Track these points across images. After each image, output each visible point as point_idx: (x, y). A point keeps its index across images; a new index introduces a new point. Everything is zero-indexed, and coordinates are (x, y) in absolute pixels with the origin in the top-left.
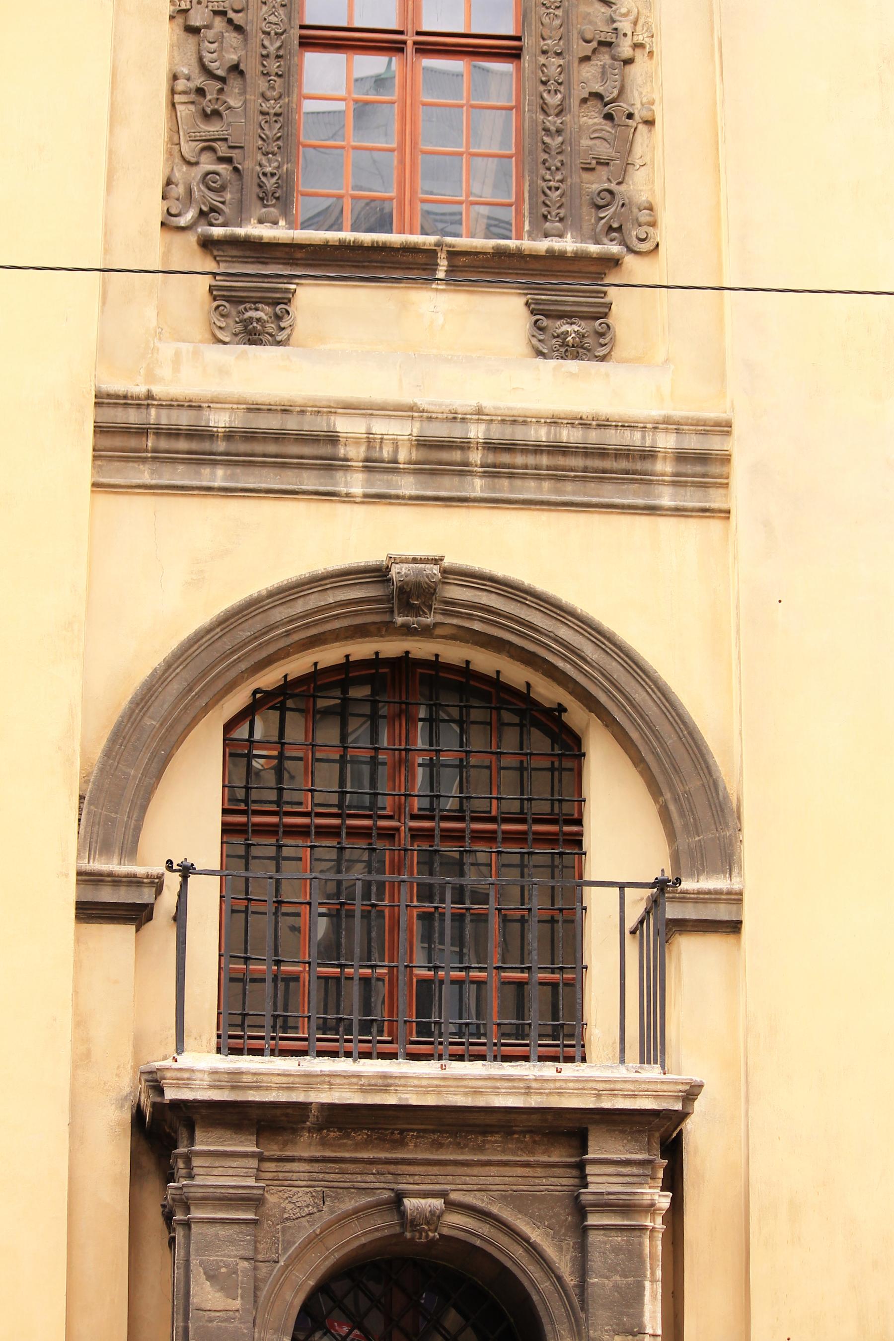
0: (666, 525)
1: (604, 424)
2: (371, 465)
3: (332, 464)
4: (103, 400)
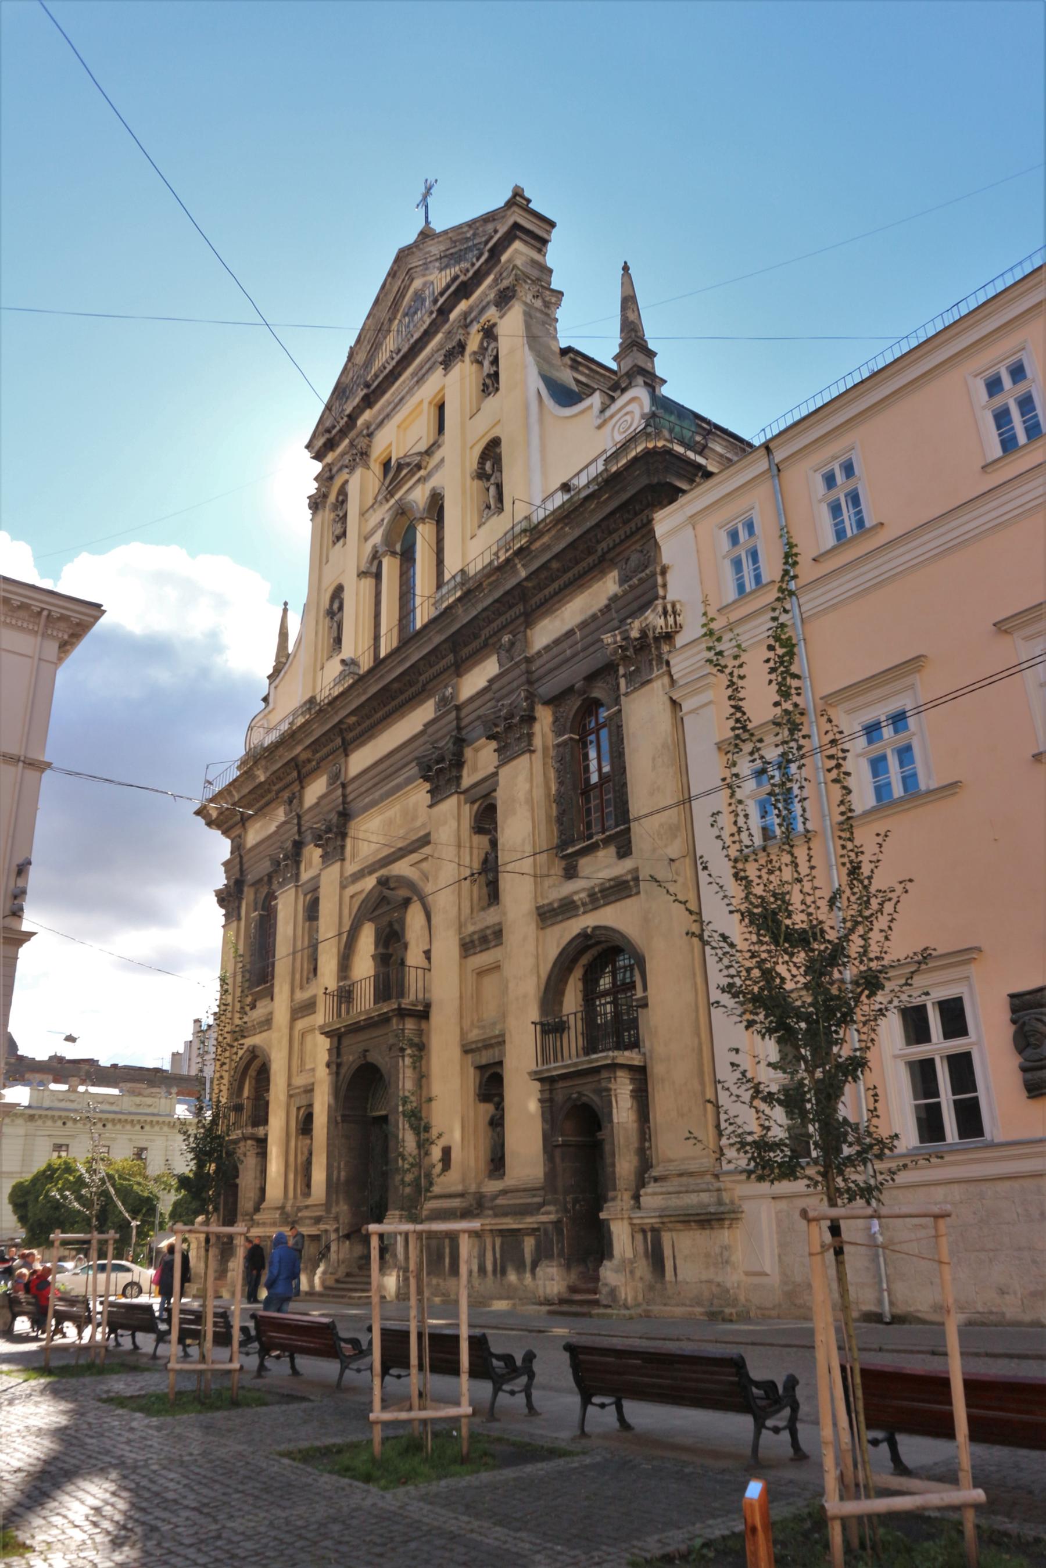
3: (577, 907)
4: (538, 908)
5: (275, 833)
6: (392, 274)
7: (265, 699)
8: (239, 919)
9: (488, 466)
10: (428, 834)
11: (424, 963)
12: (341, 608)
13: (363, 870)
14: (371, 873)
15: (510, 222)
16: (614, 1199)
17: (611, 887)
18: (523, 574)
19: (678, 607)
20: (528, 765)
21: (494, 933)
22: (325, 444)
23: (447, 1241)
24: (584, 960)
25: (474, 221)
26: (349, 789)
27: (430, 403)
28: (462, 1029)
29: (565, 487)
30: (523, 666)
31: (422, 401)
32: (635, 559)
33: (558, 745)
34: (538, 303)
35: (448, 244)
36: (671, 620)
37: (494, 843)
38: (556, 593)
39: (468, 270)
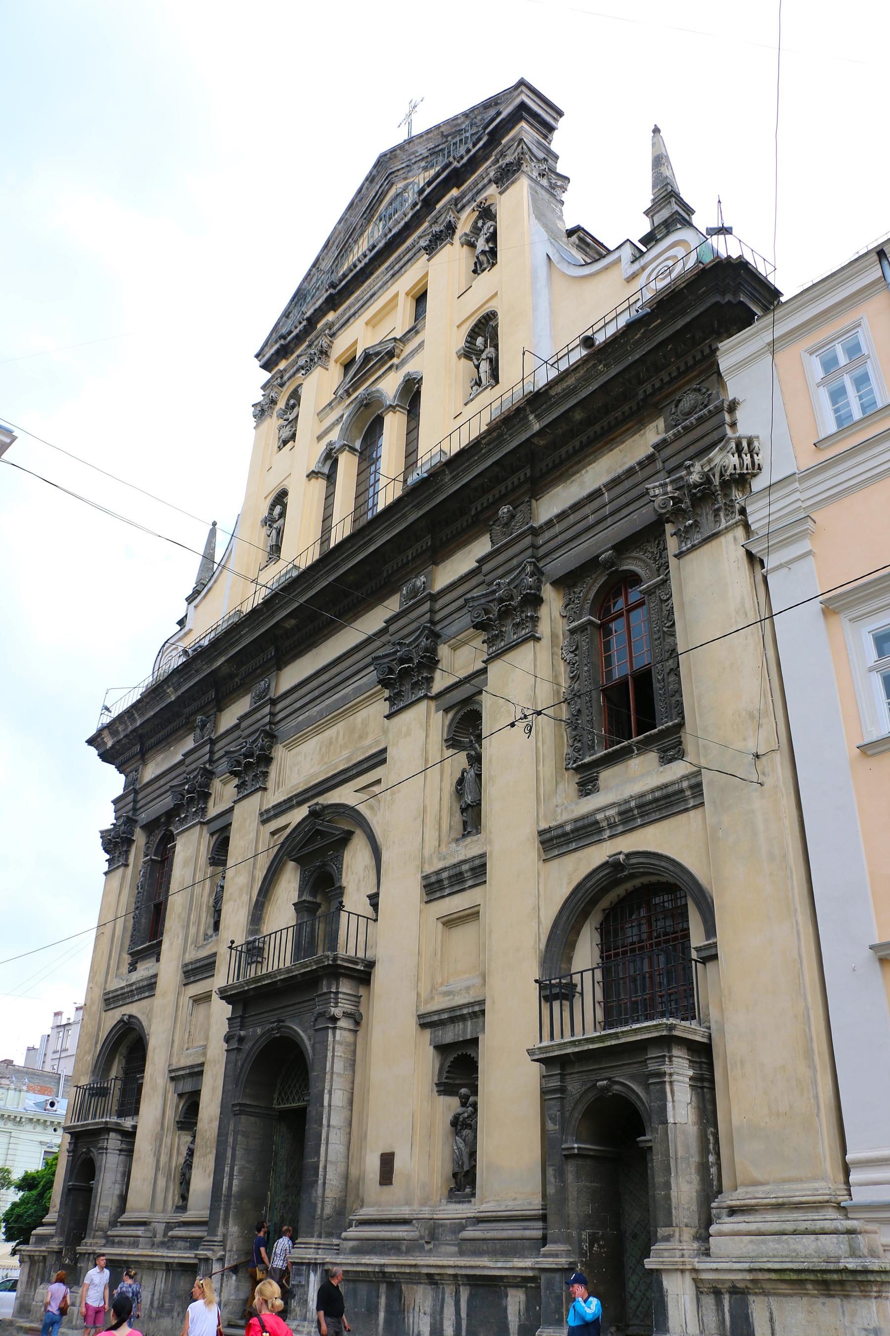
0: (692, 813)
1: (666, 786)
2: (611, 826)
3: (601, 830)
4: (541, 833)
5: (181, 763)
6: (370, 179)
7: (181, 623)
8: (127, 865)
9: (480, 341)
10: (384, 750)
11: (369, 911)
12: (282, 515)
13: (290, 799)
14: (300, 804)
15: (517, 102)
16: (667, 1239)
17: (656, 800)
18: (536, 427)
19: (756, 444)
20: (532, 655)
21: (472, 869)
22: (277, 352)
23: (383, 1288)
24: (605, 903)
25: (473, 110)
26: (279, 706)
27: (407, 294)
28: (418, 994)
29: (588, 342)
30: (528, 540)
31: (397, 295)
32: (688, 401)
33: (572, 632)
34: (544, 182)
35: (440, 140)
36: (747, 459)
37: (476, 760)
38: (576, 452)
39: (462, 157)
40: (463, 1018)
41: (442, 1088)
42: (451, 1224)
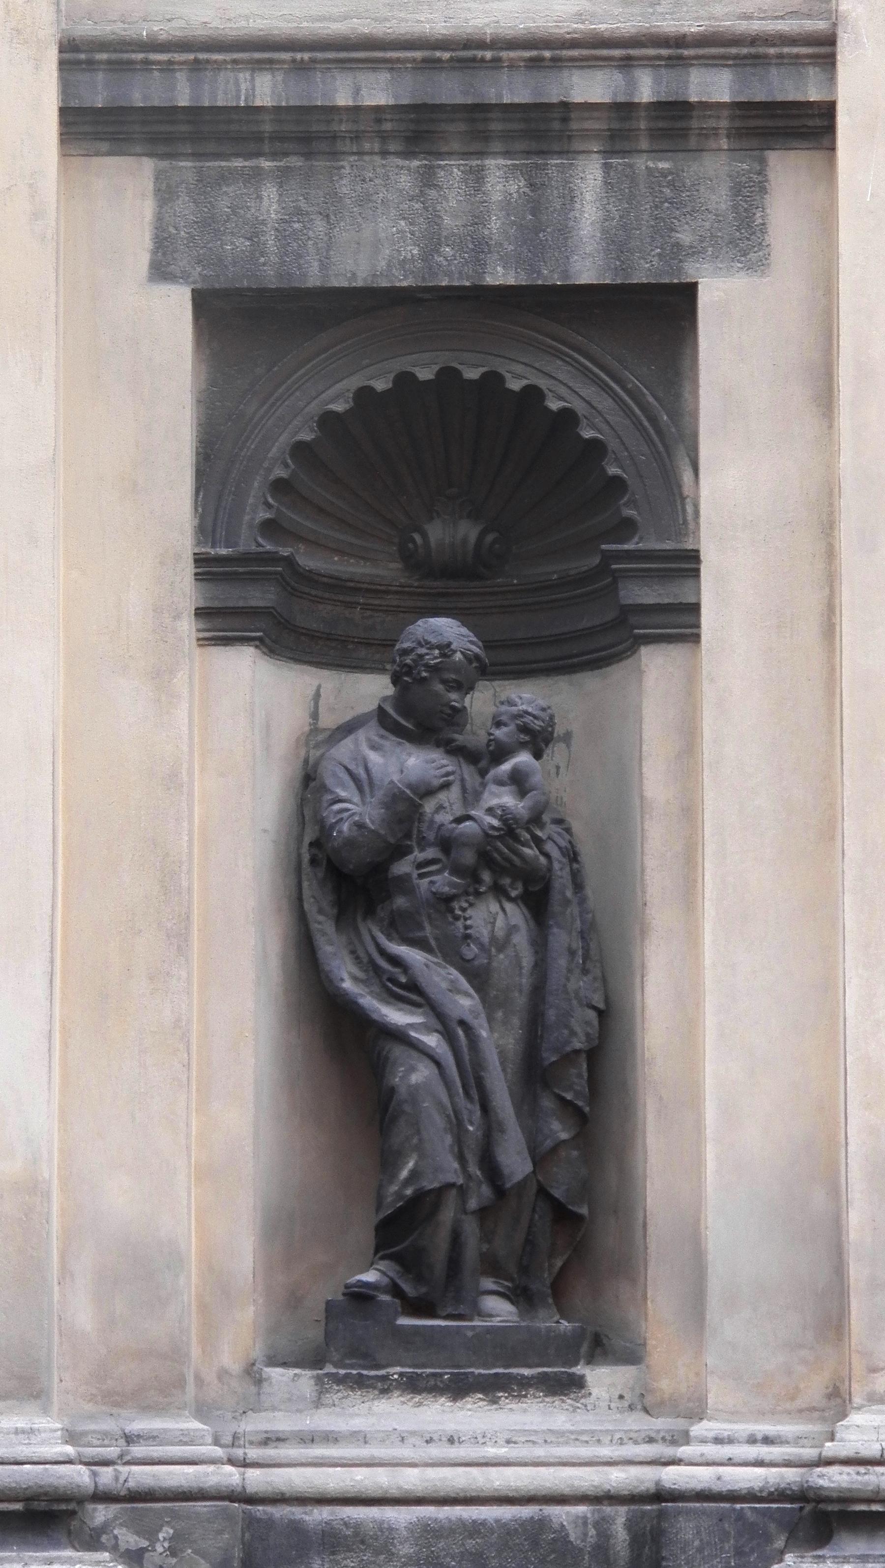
40: (542, 130)
41: (259, 597)
42: (428, 1532)
